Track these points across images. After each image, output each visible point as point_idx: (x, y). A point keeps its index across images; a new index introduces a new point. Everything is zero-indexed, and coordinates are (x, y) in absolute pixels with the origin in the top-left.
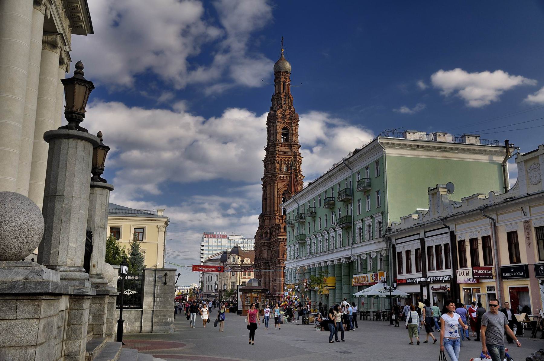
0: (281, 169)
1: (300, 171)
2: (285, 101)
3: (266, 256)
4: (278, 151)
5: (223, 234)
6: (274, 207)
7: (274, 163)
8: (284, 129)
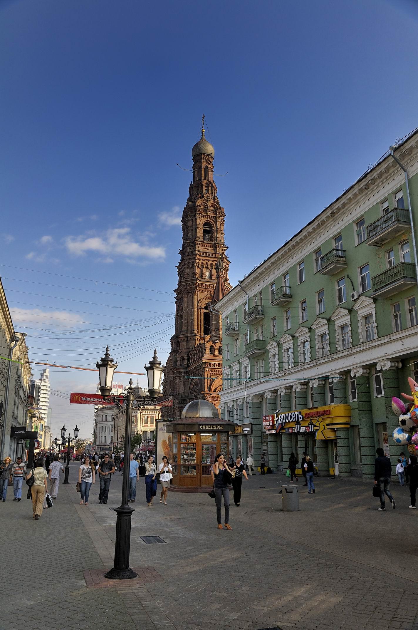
0: (202, 275)
1: (227, 279)
2: (207, 190)
3: (181, 391)
4: (199, 251)
5: (119, 384)
6: (192, 323)
7: (193, 266)
8: (206, 224)
